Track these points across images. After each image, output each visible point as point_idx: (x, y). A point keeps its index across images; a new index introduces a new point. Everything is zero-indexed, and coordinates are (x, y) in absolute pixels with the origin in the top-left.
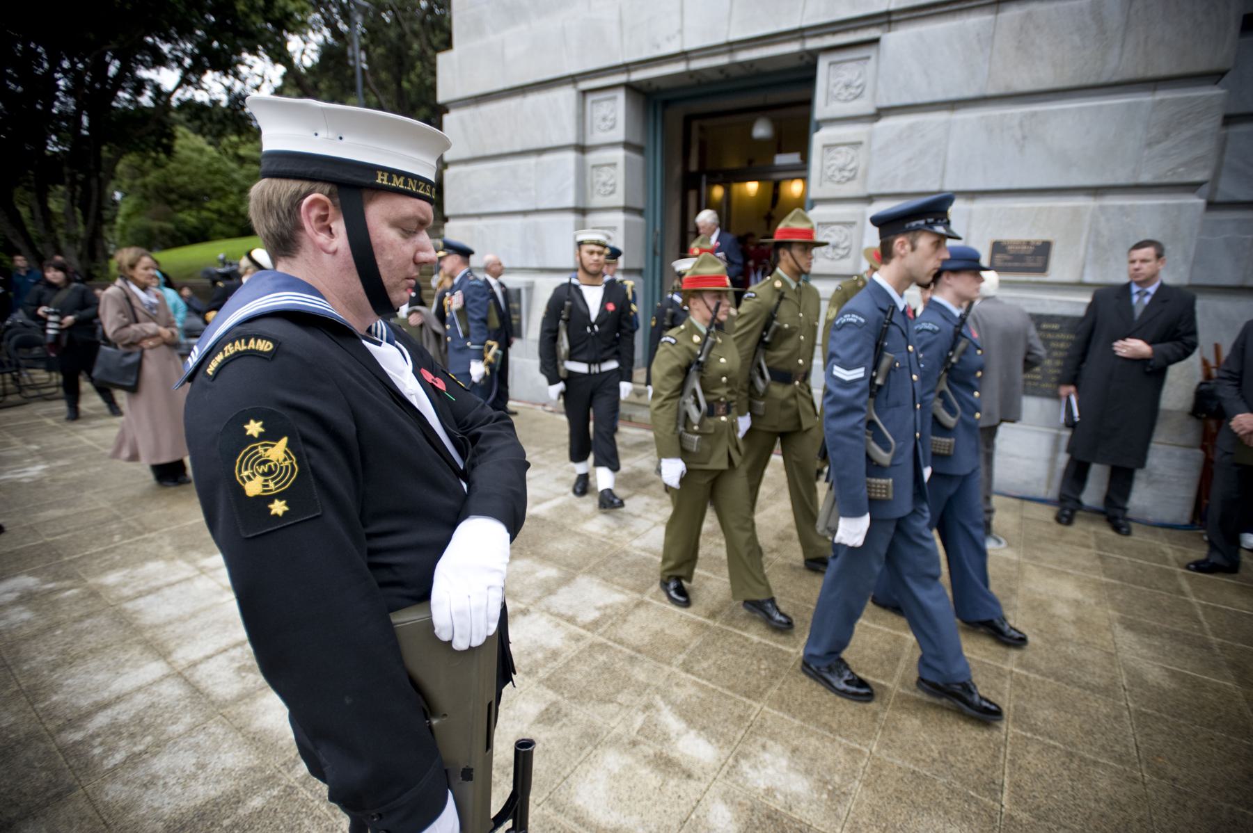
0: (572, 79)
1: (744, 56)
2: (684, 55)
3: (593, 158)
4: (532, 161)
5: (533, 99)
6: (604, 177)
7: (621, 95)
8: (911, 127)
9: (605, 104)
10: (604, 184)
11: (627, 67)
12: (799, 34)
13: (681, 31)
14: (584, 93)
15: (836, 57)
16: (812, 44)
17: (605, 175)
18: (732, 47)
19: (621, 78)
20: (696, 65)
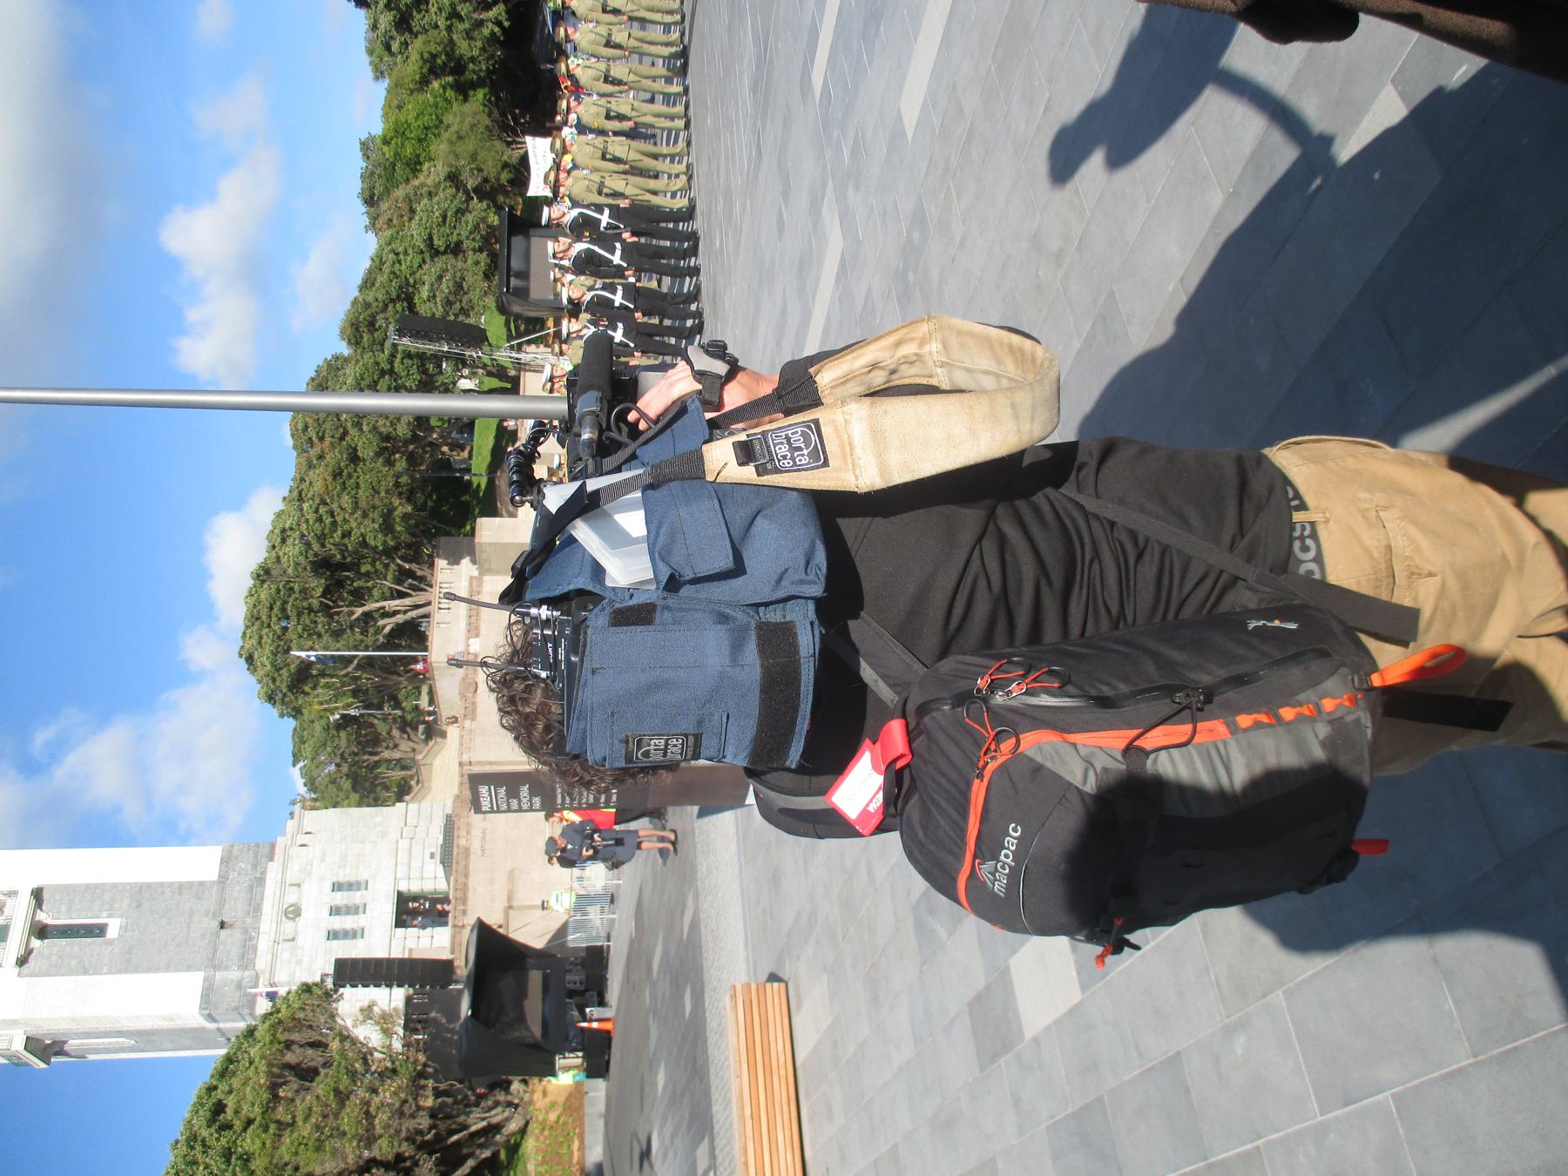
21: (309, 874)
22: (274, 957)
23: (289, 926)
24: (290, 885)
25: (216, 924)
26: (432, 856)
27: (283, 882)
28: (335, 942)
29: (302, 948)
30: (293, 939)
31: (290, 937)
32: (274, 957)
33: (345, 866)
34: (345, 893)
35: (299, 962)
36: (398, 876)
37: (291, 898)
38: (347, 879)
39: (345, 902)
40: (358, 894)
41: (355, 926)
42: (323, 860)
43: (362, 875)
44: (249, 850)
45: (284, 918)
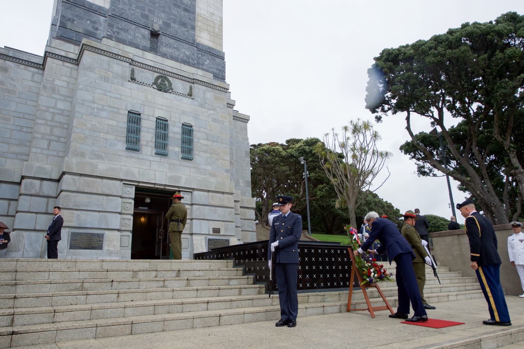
0: (122, 180)
1: (167, 188)
2: (155, 184)
3: (124, 200)
4: (105, 197)
5: (104, 180)
6: (127, 206)
7: (134, 188)
8: (199, 207)
9: (129, 188)
10: (127, 208)
11: (139, 182)
12: (179, 187)
13: (155, 179)
14: (124, 184)
15: (184, 193)
16: (180, 189)
17: (128, 205)
18: (165, 185)
19: (137, 184)
20: (156, 186)
21: (202, 105)
22: (115, 56)
23: (150, 77)
24: (191, 88)
25: (156, 28)
26: (216, 231)
27: (194, 81)
28: (125, 119)
29: (122, 86)
30: (133, 79)
31: (136, 76)
32: (115, 56)
33: (208, 140)
34: (179, 136)
35: (106, 79)
36: (195, 193)
37: (178, 85)
38: (195, 140)
39: (170, 135)
40: (178, 149)
41: (143, 142)
42: (214, 120)
43: (199, 156)
44: (220, 71)
45: (157, 75)
